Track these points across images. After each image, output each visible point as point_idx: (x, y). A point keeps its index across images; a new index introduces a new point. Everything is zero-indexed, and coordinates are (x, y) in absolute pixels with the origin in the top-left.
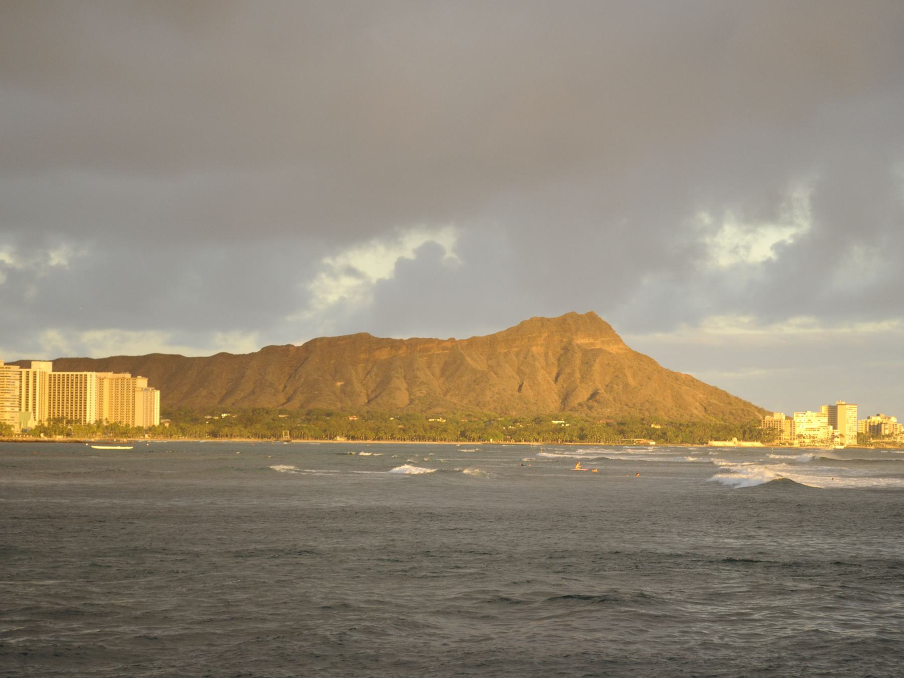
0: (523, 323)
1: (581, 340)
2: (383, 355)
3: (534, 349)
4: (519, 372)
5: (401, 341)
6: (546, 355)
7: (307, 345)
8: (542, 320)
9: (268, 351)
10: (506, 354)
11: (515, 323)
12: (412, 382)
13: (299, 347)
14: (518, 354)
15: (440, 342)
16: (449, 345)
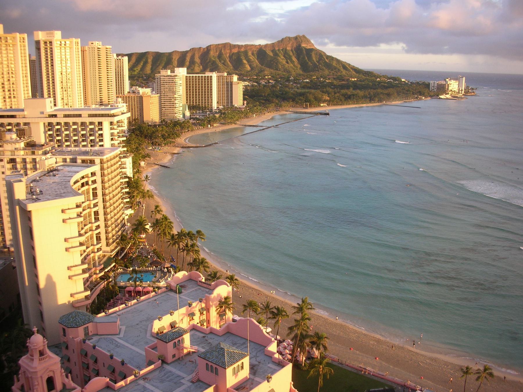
0: (283, 39)
1: (303, 45)
2: (235, 51)
3: (288, 48)
4: (284, 56)
5: (242, 45)
6: (292, 50)
7: (207, 47)
8: (289, 38)
9: (193, 50)
10: (279, 50)
11: (281, 39)
12: (249, 61)
13: (204, 49)
14: (282, 50)
15: (256, 46)
16: (259, 47)
